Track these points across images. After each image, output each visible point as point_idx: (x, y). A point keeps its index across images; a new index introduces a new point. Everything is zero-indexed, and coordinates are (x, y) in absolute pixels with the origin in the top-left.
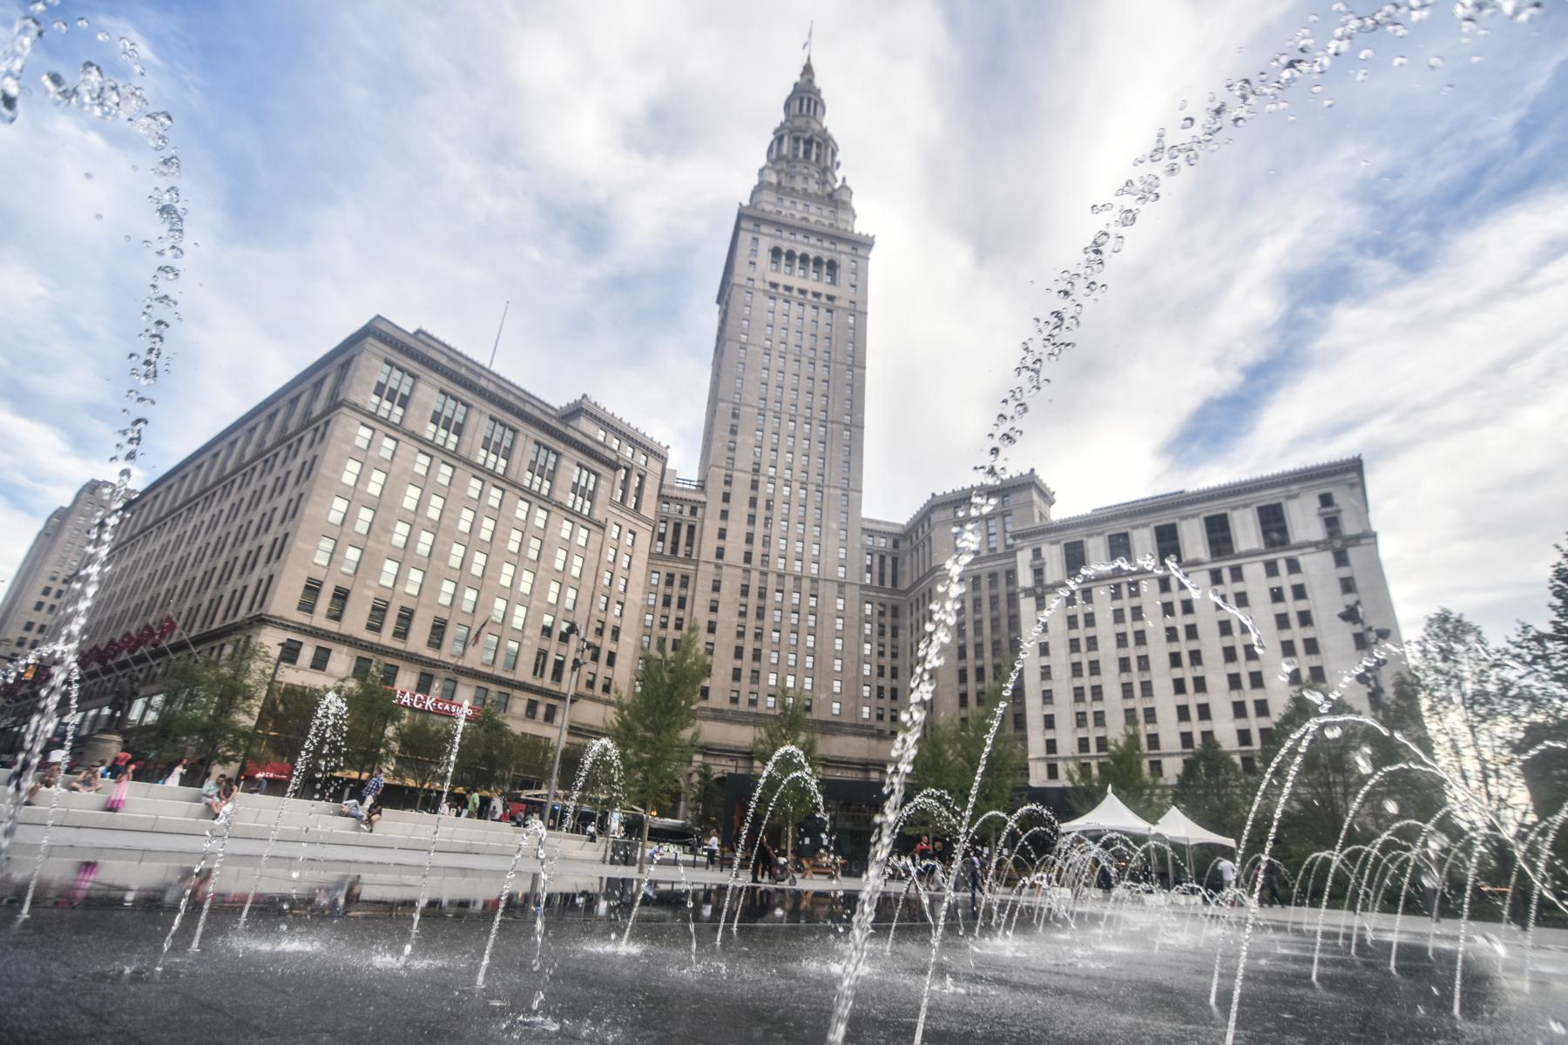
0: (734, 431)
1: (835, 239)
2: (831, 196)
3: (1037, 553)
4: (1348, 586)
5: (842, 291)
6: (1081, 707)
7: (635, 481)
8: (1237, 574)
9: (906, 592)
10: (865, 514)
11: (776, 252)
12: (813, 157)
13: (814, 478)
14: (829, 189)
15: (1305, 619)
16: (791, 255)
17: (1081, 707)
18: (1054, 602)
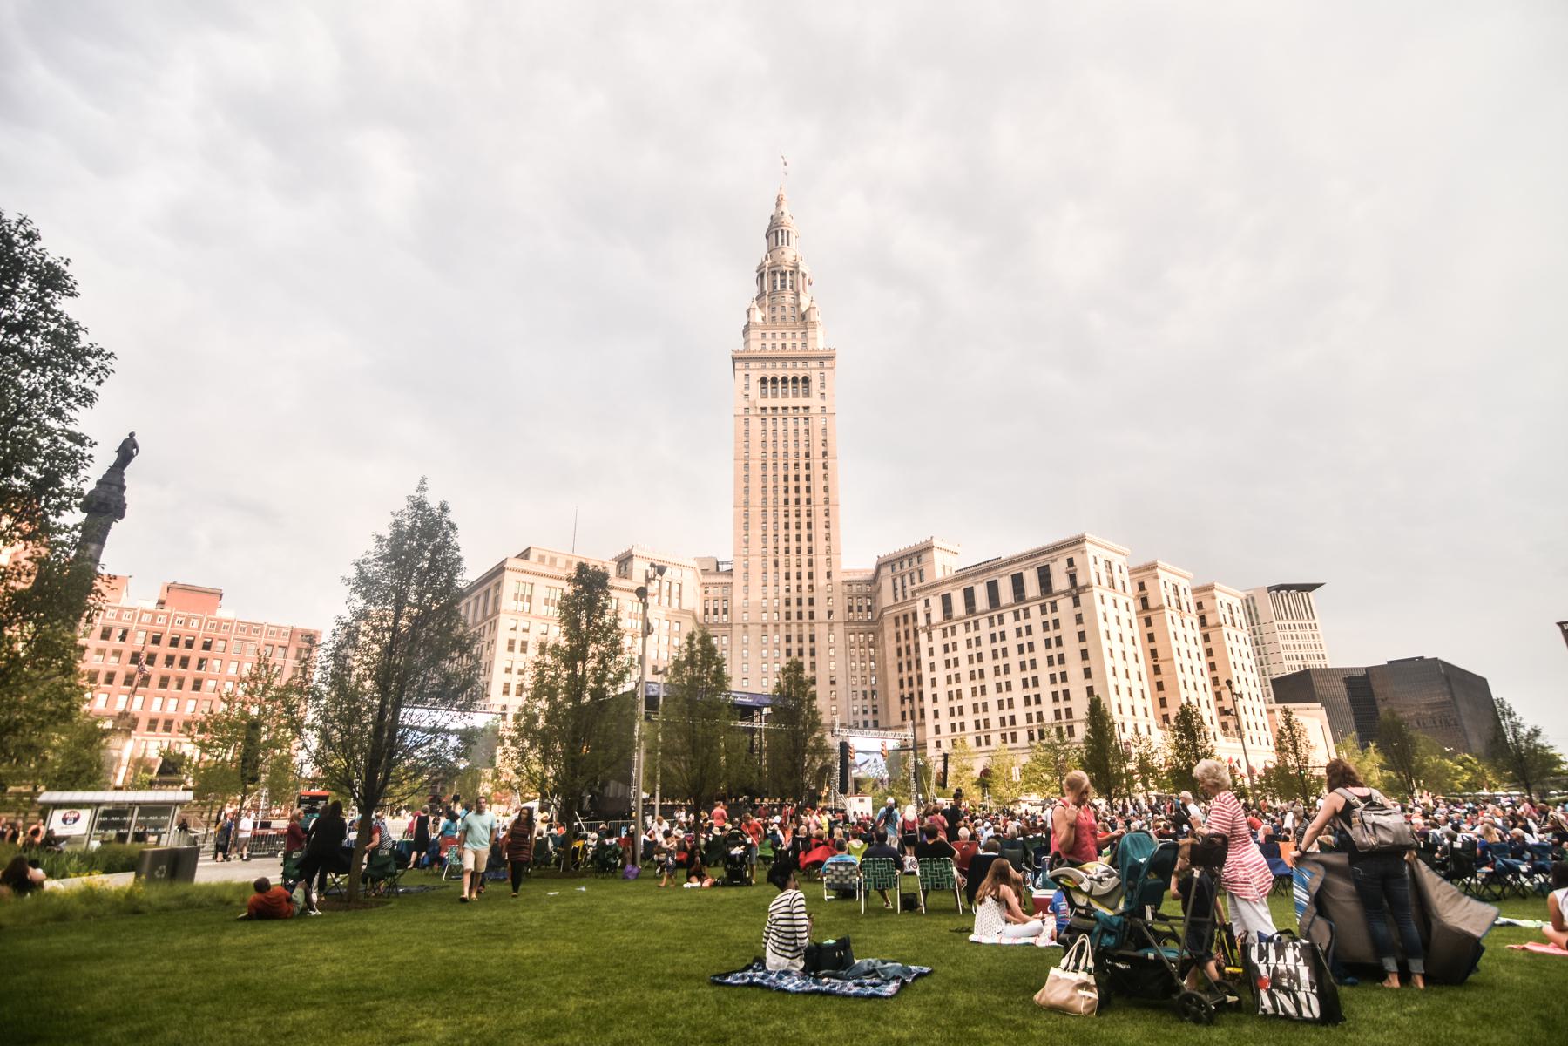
0: (746, 528)
1: (805, 359)
2: (803, 316)
3: (927, 603)
4: (1079, 619)
5: (814, 402)
6: (952, 704)
7: (675, 588)
8: (1026, 611)
9: (875, 622)
10: (845, 567)
11: (764, 380)
12: (788, 284)
13: (804, 550)
14: (803, 309)
15: (1059, 642)
16: (774, 380)
17: (952, 704)
18: (937, 634)
